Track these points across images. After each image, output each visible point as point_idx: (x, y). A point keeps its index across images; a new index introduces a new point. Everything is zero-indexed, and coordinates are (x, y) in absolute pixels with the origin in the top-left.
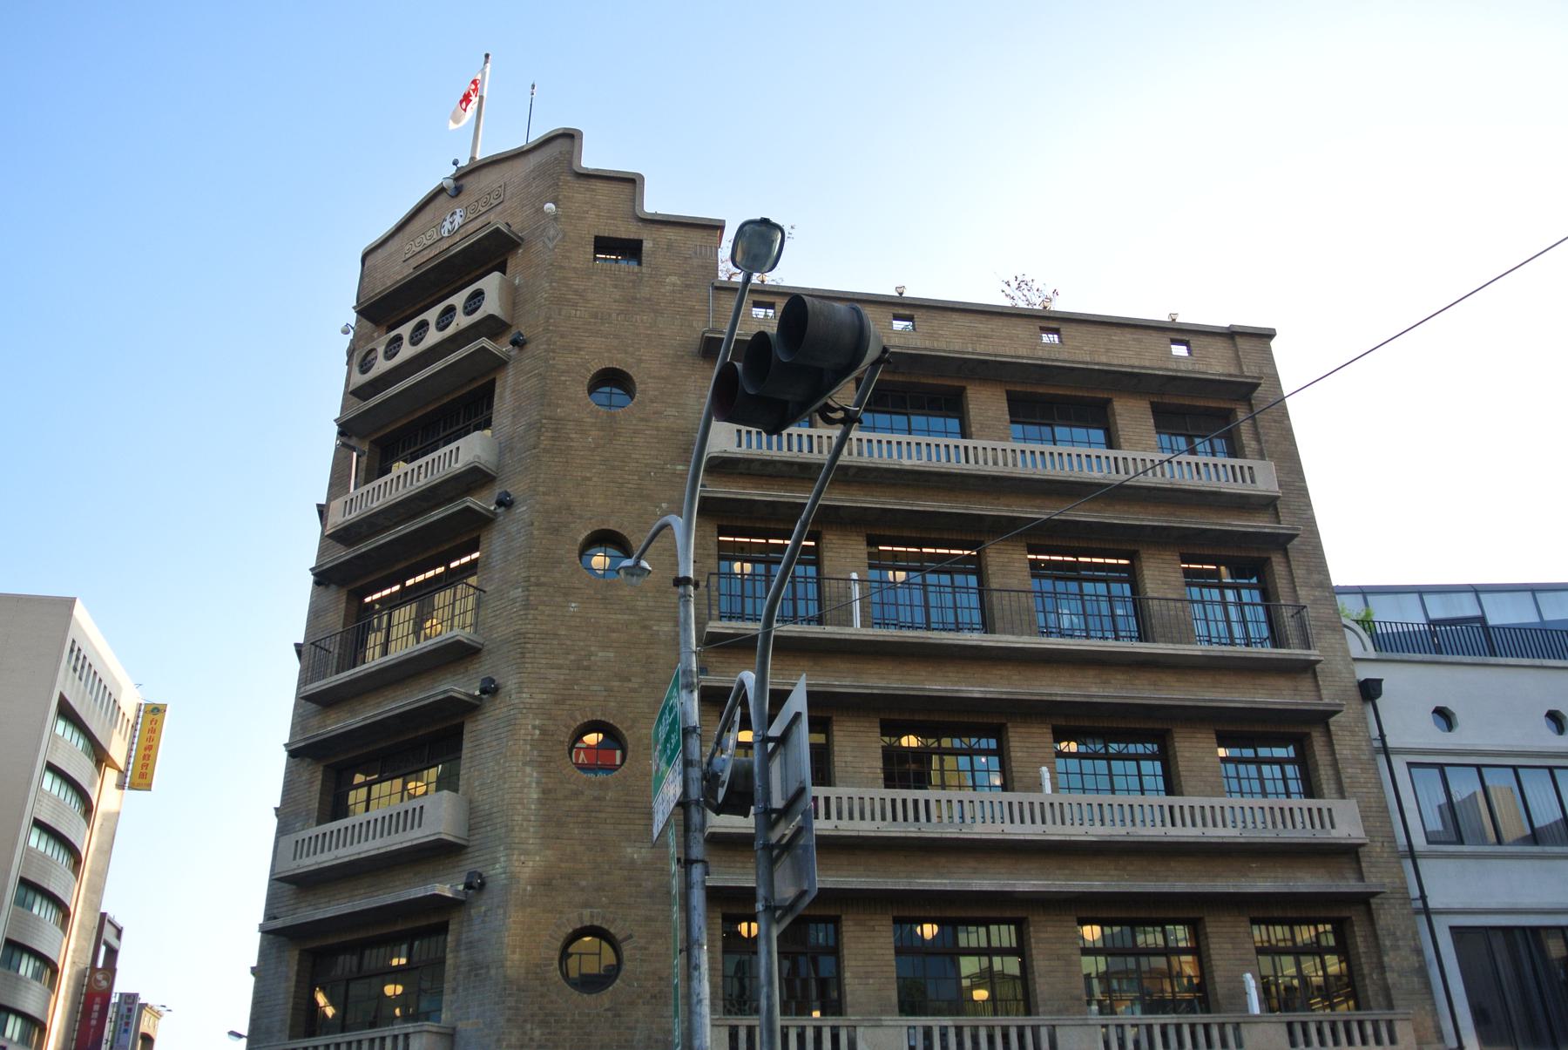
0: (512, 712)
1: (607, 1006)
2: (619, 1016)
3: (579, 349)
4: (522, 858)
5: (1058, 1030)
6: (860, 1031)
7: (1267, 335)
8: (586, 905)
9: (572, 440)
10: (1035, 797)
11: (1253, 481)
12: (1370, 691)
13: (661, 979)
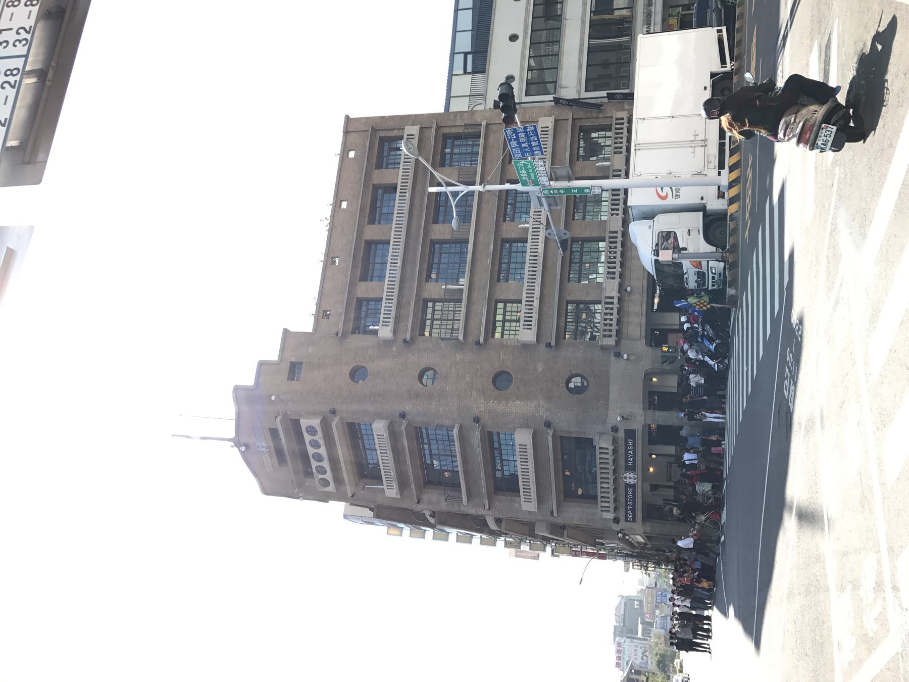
1: (593, 379)
2: (597, 375)
4: (541, 407)
5: (611, 230)
6: (607, 295)
8: (558, 385)
9: (380, 389)
10: (530, 230)
11: (413, 135)
13: (585, 361)
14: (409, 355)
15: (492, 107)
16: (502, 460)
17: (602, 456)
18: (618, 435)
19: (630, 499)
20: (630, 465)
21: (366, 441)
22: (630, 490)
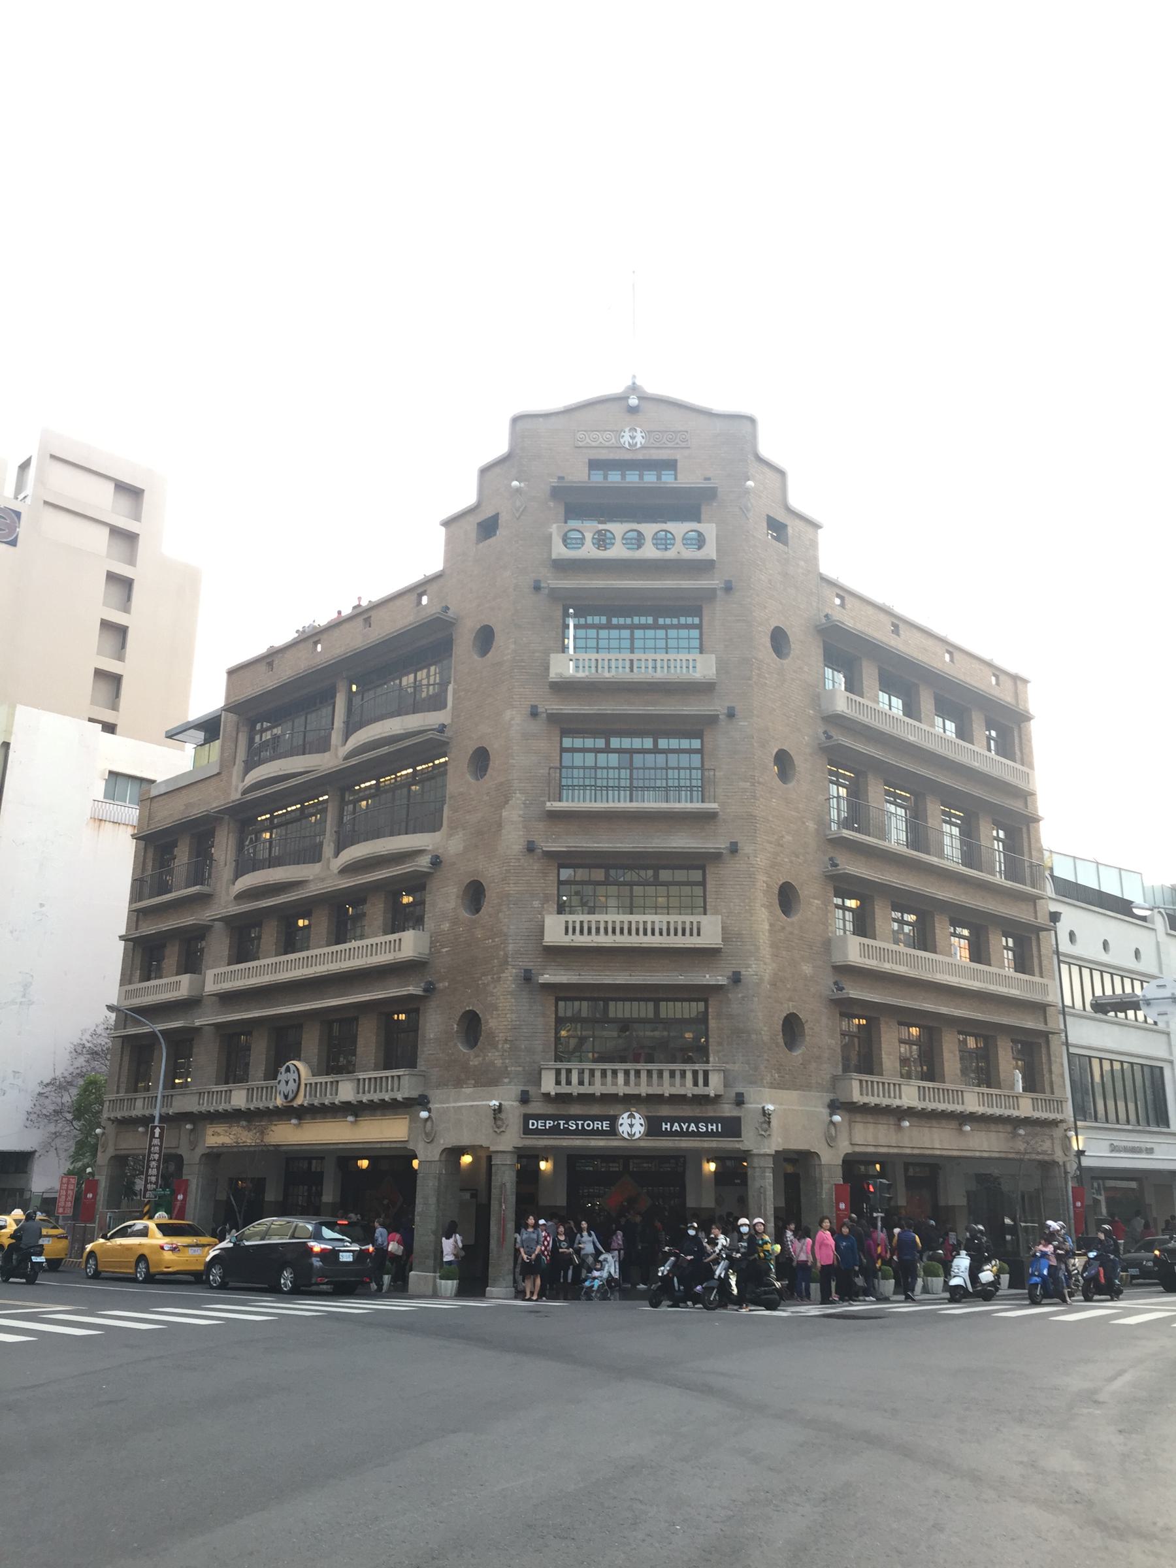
0: (751, 869)
3: (765, 607)
6: (902, 1086)
7: (1025, 682)
9: (766, 678)
12: (1055, 917)
14: (806, 738)
15: (1052, 910)
16: (631, 884)
17: (689, 1075)
18: (726, 1105)
19: (583, 1125)
20: (664, 1126)
21: (650, 633)
22: (605, 1125)
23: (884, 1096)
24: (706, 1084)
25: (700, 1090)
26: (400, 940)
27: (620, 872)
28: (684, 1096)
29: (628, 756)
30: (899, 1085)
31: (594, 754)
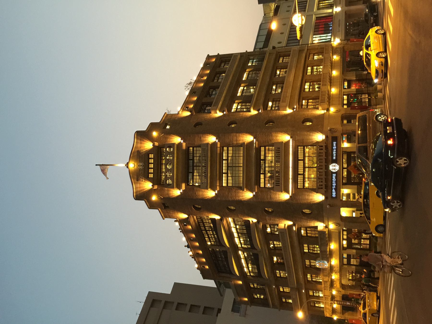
6: (322, 90)
12: (274, 48)
15: (272, 48)
23: (325, 96)
24: (322, 146)
25: (324, 148)
26: (281, 232)
27: (261, 170)
28: (326, 153)
29: (229, 168)
30: (322, 91)
31: (228, 177)
